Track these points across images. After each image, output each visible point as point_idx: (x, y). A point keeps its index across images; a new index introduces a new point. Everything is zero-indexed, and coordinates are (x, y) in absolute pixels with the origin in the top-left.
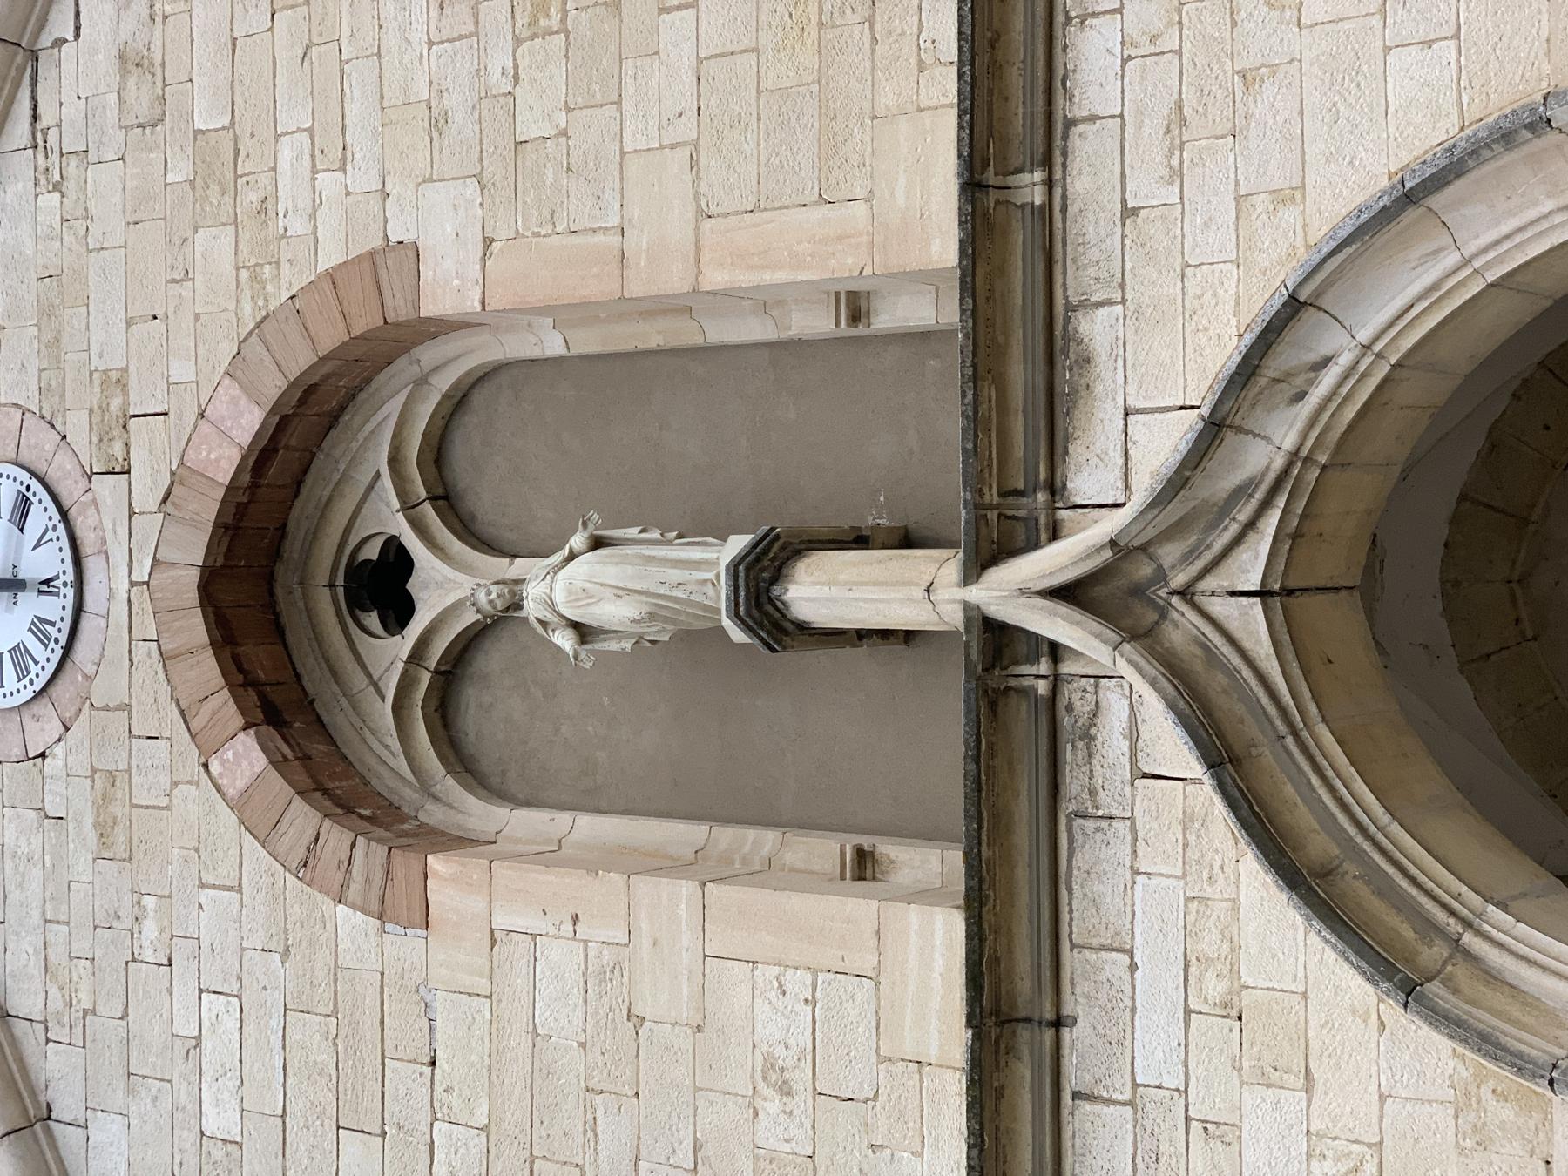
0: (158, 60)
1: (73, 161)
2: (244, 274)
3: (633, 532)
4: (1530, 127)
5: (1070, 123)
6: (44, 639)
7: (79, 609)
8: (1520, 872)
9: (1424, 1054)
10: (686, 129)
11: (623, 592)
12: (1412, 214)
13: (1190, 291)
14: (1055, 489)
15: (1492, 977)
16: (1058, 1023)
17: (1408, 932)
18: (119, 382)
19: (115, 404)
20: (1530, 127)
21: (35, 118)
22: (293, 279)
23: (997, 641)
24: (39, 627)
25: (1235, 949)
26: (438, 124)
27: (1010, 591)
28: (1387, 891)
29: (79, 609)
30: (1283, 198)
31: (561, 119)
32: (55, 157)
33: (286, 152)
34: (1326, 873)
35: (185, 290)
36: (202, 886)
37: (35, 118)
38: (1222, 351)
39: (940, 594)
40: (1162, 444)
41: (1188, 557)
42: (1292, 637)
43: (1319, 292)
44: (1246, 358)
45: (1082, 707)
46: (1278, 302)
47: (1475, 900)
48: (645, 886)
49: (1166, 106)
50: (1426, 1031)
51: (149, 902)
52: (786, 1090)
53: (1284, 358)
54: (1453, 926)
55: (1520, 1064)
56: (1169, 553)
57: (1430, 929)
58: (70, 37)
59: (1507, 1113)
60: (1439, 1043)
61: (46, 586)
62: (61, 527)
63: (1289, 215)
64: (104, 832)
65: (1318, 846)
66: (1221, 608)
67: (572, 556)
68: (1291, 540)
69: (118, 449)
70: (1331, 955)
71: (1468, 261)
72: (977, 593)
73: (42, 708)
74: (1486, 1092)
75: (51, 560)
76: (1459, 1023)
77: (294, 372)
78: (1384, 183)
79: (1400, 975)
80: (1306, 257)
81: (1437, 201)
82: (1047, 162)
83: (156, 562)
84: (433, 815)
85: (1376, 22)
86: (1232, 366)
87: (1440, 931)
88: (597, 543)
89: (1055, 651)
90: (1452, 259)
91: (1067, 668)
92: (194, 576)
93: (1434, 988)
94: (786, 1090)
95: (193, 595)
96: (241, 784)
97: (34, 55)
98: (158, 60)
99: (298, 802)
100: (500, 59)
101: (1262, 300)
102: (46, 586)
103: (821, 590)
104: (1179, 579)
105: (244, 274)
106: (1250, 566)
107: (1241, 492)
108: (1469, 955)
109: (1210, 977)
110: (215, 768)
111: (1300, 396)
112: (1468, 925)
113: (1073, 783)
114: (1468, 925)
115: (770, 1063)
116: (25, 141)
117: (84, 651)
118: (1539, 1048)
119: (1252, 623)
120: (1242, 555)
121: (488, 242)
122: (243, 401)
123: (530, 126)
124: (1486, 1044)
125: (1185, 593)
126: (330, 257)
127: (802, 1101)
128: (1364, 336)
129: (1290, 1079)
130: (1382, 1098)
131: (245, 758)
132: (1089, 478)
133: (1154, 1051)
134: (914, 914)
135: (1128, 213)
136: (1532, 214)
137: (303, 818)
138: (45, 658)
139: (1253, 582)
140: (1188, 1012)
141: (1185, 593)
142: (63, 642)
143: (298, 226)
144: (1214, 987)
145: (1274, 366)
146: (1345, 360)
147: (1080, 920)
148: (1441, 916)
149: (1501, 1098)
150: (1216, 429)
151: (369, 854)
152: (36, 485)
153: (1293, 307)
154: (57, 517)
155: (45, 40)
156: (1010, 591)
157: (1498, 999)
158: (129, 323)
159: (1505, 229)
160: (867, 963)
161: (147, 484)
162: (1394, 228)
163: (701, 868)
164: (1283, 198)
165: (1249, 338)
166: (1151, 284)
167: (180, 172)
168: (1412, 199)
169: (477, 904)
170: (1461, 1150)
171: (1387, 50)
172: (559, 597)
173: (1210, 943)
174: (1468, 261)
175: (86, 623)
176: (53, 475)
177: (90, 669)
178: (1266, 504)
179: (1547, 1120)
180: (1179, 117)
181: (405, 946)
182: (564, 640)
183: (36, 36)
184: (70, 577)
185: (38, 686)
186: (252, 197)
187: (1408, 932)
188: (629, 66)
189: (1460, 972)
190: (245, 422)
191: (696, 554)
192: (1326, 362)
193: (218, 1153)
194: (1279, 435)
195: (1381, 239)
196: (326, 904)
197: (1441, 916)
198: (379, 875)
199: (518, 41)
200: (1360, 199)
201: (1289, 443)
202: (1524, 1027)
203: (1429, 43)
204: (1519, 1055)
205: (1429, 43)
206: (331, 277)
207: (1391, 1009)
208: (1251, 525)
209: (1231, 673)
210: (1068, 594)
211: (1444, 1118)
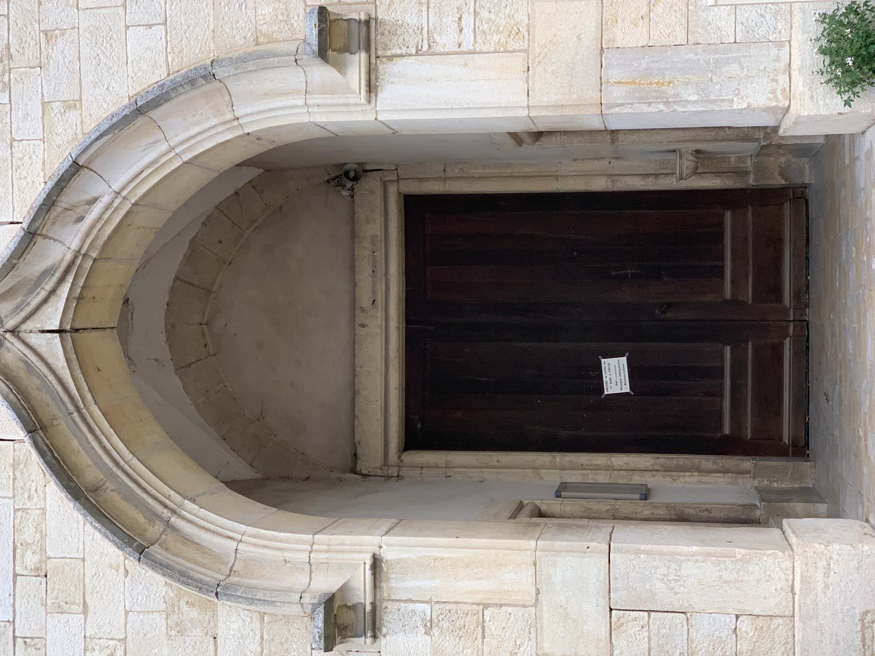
4: (204, 77)
8: (203, 481)
9: (153, 585)
12: (141, 120)
13: (17, 155)
15: (187, 540)
17: (141, 519)
20: (204, 77)
25: (43, 537)
28: (129, 497)
30: (72, 105)
34: (96, 489)
38: (35, 191)
42: (78, 357)
43: (90, 160)
44: (49, 195)
46: (67, 164)
47: (177, 498)
50: (150, 573)
53: (70, 197)
54: (166, 513)
55: (200, 586)
57: (152, 516)
59: (194, 613)
60: (157, 580)
65: (92, 474)
66: (35, 340)
68: (77, 300)
70: (98, 536)
71: (172, 149)
74: (182, 603)
76: (168, 567)
78: (126, 101)
79: (136, 544)
80: (82, 140)
81: (155, 114)
85: (121, 10)
86: (40, 200)
87: (159, 517)
90: (164, 147)
93: (155, 549)
101: (58, 164)
104: (10, 324)
106: (53, 315)
107: (47, 273)
108: (174, 529)
109: (29, 553)
111: (81, 219)
112: (174, 512)
114: (174, 512)
118: (210, 576)
119: (54, 349)
120: (48, 309)
124: (183, 577)
125: (14, 331)
128: (116, 186)
129: (75, 608)
130: (127, 613)
136: (206, 125)
139: (55, 326)
140: (15, 575)
141: (14, 331)
144: (31, 560)
145: (66, 200)
146: (106, 199)
148: (159, 508)
149: (190, 606)
150: (31, 236)
153: (75, 168)
157: (189, 551)
159: (192, 132)
162: (132, 128)
164: (72, 105)
165: (50, 184)
168: (141, 111)
170: (169, 637)
171: (127, 27)
173: (29, 535)
174: (172, 149)
178: (62, 280)
179: (215, 615)
187: (141, 519)
189: (169, 538)
192: (95, 200)
194: (66, 242)
195: (126, 132)
197: (159, 508)
200: (113, 110)
201: (75, 246)
202: (203, 566)
203: (150, 26)
204: (200, 581)
205: (150, 26)
207: (132, 564)
208: (53, 292)
209: (42, 378)
211: (160, 621)
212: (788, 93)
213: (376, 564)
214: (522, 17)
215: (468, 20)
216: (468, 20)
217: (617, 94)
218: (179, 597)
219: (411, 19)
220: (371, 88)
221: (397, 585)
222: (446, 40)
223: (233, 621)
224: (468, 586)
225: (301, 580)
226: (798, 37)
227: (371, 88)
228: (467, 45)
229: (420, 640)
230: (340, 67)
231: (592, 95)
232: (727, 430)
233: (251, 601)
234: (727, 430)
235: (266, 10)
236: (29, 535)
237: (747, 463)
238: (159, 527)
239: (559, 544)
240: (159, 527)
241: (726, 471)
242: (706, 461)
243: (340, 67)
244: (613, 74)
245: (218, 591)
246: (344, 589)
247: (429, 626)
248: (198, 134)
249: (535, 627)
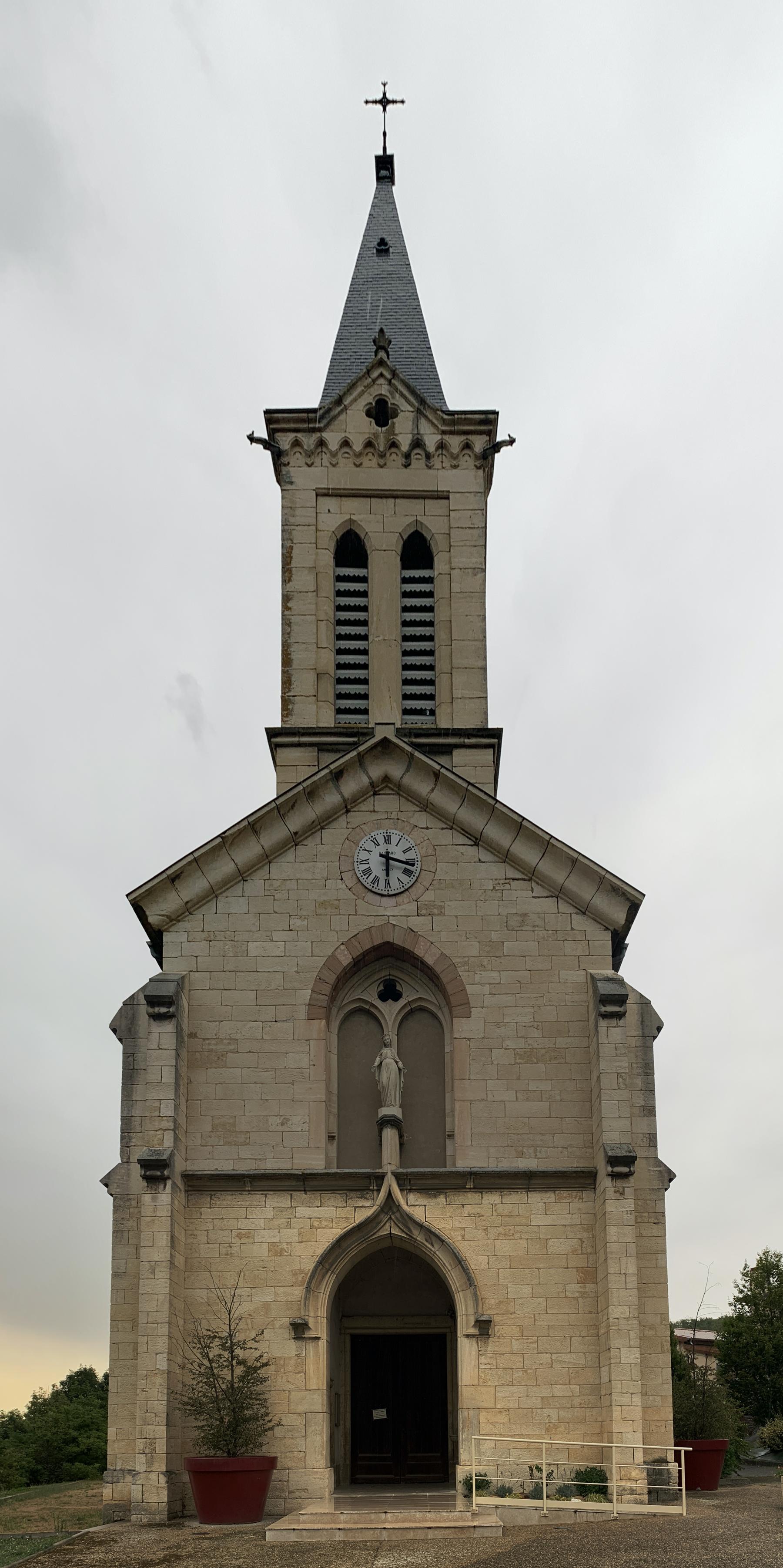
0: (523, 928)
1: (500, 895)
2: (466, 959)
3: (402, 1079)
5: (482, 1193)
6: (373, 882)
7: (382, 895)
9: (309, 1266)
10: (490, 1098)
11: (389, 1078)
14: (410, 1190)
16: (305, 1191)
18: (441, 914)
19: (435, 911)
21: (514, 879)
22: (464, 975)
23: (380, 1178)
24: (376, 880)
26: (498, 1025)
27: (391, 1183)
29: (382, 895)
31: (495, 1063)
32: (502, 888)
33: (495, 974)
35: (464, 938)
36: (312, 942)
37: (514, 879)
39: (389, 1166)
40: (418, 1213)
41: (397, 1218)
45: (368, 1196)
48: (323, 1085)
49: (483, 1213)
51: (306, 922)
52: (282, 1124)
55: (309, 1283)
56: (398, 1215)
58: (534, 895)
59: (300, 1279)
61: (388, 883)
62: (403, 889)
63: (460, 1238)
64: (323, 904)
65: (344, 1245)
66: (388, 1225)
67: (397, 1062)
69: (424, 912)
70: (325, 1247)
72: (389, 1174)
73: (355, 880)
75: (395, 887)
77: (441, 976)
82: (474, 1188)
83: (394, 925)
84: (334, 1011)
88: (400, 1070)
89: (379, 1190)
91: (375, 1193)
92: (391, 940)
94: (282, 1124)
95: (386, 940)
96: (338, 956)
97: (530, 880)
98: (523, 928)
99: (335, 976)
100: (510, 1044)
102: (388, 883)
103: (390, 1135)
104: (393, 1217)
105: (466, 959)
108: (327, 1272)
110: (343, 947)
113: (353, 1194)
115: (288, 1120)
116: (508, 876)
117: (370, 895)
119: (384, 1232)
120: (397, 1230)
121: (469, 1039)
122: (435, 958)
123: (495, 1052)
125: (390, 1218)
126: (470, 989)
127: (280, 1128)
131: (345, 959)
132: (412, 1197)
133: (302, 1211)
134: (323, 1156)
135: (463, 1205)
137: (332, 978)
138: (368, 881)
139: (393, 1232)
141: (390, 1218)
142: (374, 890)
143: (477, 978)
144: (316, 1224)
145: (433, 1238)
147: (326, 1196)
150: (421, 1226)
151: (324, 1000)
152: (415, 878)
153: (443, 1241)
154: (406, 887)
155: (534, 884)
156: (391, 1183)
158: (456, 917)
160: (312, 1145)
161: (415, 922)
163: (328, 1102)
164: (463, 1236)
166: (449, 1210)
167: (494, 936)
169: (315, 1036)
172: (388, 1060)
175: (378, 897)
176: (418, 884)
177: (366, 899)
178: (407, 1234)
179: (300, 1286)
180: (480, 1216)
181: (302, 1012)
182: (378, 1060)
183: (535, 881)
184: (391, 893)
185: (361, 879)
186: (485, 963)
188: (505, 1082)
189: (324, 1271)
190: (430, 960)
191: (397, 1099)
192: (433, 1246)
193: (244, 948)
194: (420, 1237)
196: (311, 986)
198: (320, 1004)
199: (514, 1050)
206: (464, 990)
209: (375, 1228)
210: (390, 1195)
211: (297, 1267)
212: (465, 1465)
213: (318, 1338)
214: (489, 1383)
215: (488, 1366)
216: (488, 1366)
217: (466, 1413)
218: (306, 1274)
219: (489, 1349)
220: (468, 1336)
221: (311, 1346)
222: (483, 1360)
223: (298, 1292)
224: (311, 1368)
225: (312, 1314)
226: (481, 1467)
227: (468, 1336)
228: (481, 1366)
229: (294, 1353)
230: (474, 1326)
231: (465, 1406)
232: (360, 1455)
233: (305, 1299)
234: (360, 1455)
235: (493, 1301)
236: (324, 1223)
237: (348, 1462)
238: (327, 1267)
239: (325, 1397)
240: (327, 1267)
241: (345, 1454)
242: (349, 1447)
243: (474, 1326)
244: (471, 1412)
245: (308, 1289)
246: (310, 1328)
247: (298, 1356)
248: (454, 1279)
249: (299, 1390)
